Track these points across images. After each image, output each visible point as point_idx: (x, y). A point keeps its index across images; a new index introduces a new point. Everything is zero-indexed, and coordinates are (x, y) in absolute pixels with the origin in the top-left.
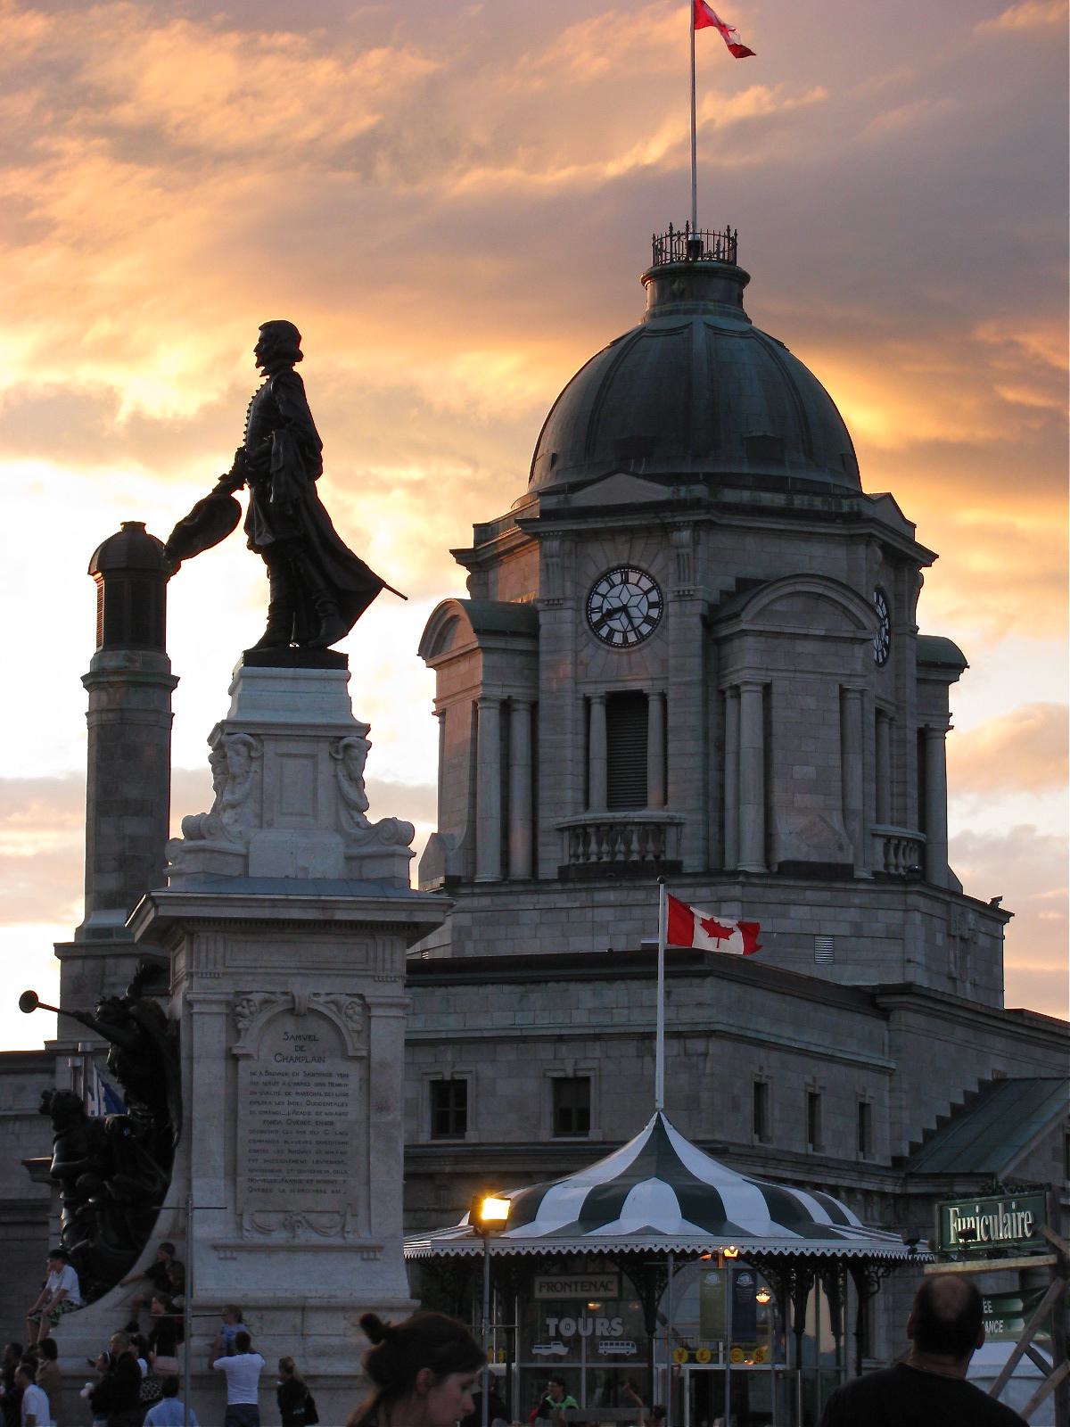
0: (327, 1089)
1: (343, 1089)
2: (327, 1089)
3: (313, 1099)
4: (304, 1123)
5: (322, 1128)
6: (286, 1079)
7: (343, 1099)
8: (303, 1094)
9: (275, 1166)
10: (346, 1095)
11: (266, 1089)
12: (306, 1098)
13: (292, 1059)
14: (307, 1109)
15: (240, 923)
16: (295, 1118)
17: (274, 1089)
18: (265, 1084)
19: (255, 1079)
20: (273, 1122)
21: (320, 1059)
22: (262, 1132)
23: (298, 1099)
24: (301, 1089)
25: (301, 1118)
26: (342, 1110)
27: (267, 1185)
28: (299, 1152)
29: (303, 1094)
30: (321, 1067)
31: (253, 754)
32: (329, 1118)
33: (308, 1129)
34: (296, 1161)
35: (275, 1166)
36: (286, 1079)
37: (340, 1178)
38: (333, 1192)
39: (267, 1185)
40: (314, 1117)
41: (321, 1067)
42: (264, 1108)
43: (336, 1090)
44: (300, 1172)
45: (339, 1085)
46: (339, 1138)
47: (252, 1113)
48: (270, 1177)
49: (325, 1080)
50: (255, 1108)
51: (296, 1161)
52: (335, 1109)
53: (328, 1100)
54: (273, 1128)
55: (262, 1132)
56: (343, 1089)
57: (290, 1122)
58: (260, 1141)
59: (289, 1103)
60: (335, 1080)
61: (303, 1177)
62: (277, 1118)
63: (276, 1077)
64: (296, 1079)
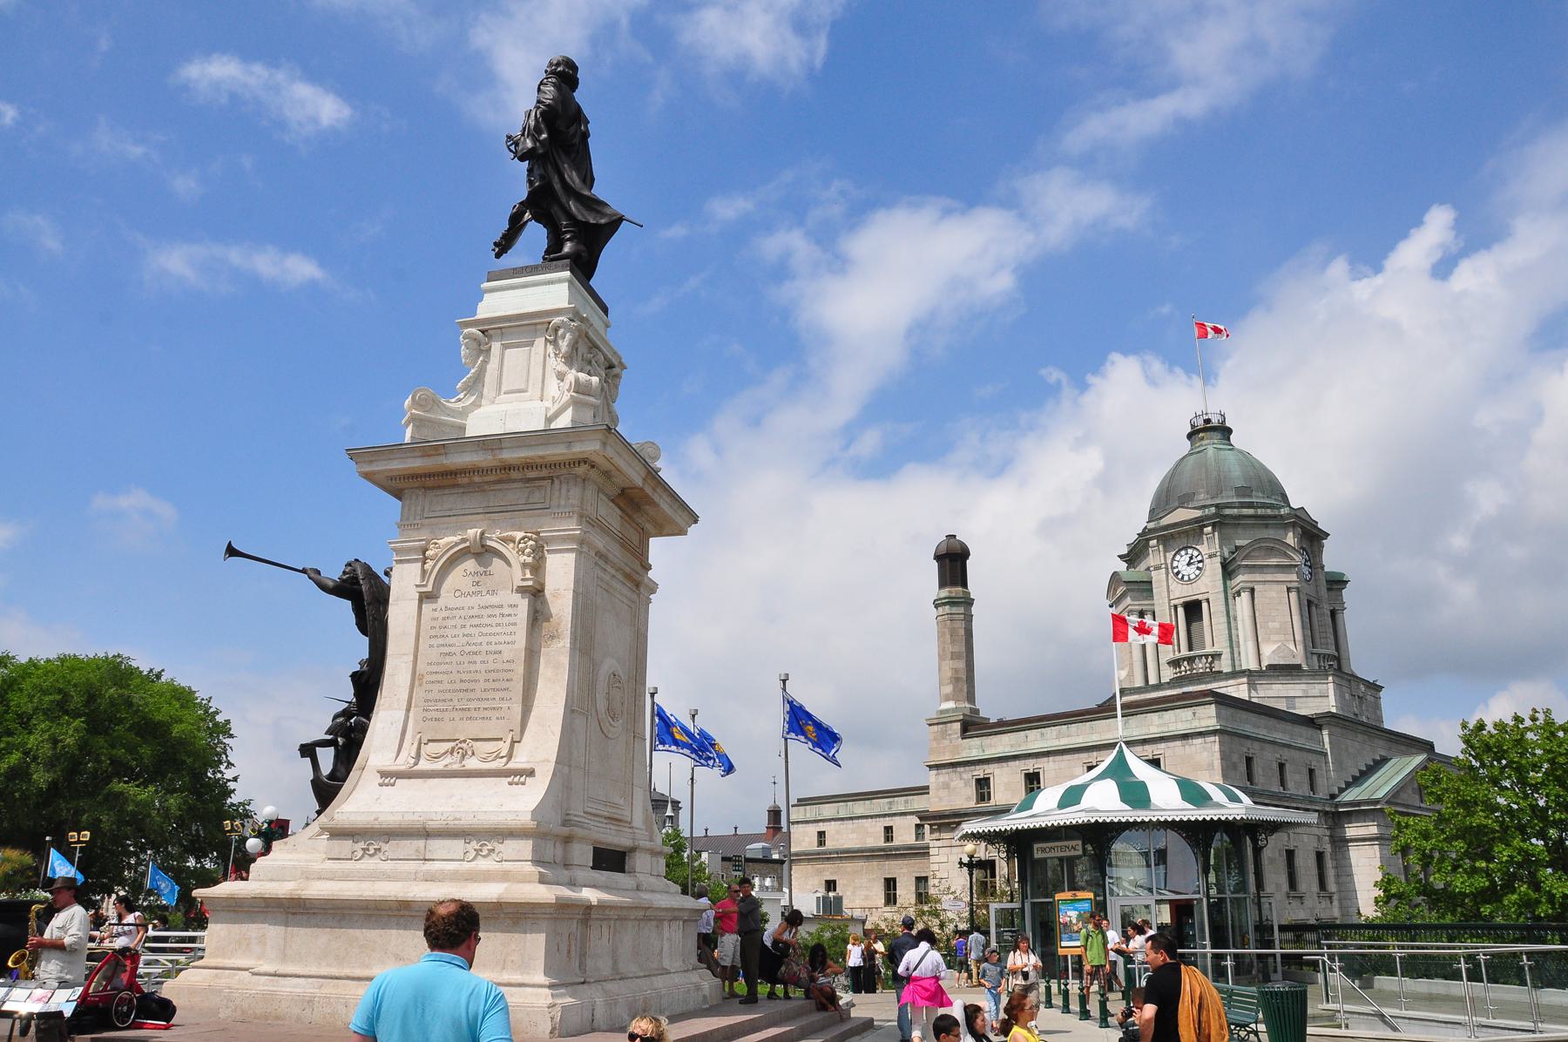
0: (498, 620)
1: (512, 619)
2: (498, 620)
3: (485, 630)
4: (475, 653)
5: (466, 659)
6: (462, 613)
7: (511, 628)
8: (476, 626)
9: (448, 696)
10: (515, 624)
11: (444, 623)
12: (479, 629)
13: (469, 594)
14: (480, 639)
15: (442, 476)
16: (467, 649)
17: (452, 622)
18: (444, 619)
19: (436, 614)
20: (449, 654)
21: (493, 592)
22: (439, 664)
23: (473, 631)
24: (475, 621)
25: (473, 648)
26: (508, 639)
27: (439, 715)
28: (470, 681)
29: (476, 626)
30: (494, 600)
31: (482, 348)
32: (499, 647)
33: (478, 658)
34: (466, 690)
35: (448, 696)
36: (462, 613)
37: (505, 705)
38: (498, 718)
39: (439, 715)
40: (485, 648)
41: (494, 600)
42: (441, 641)
43: (506, 620)
44: (469, 700)
45: (510, 615)
46: (506, 666)
47: (431, 646)
48: (440, 706)
49: (497, 611)
50: (433, 642)
51: (466, 690)
52: (502, 638)
53: (499, 630)
54: (448, 659)
55: (439, 664)
56: (512, 619)
57: (462, 653)
58: (436, 673)
59: (464, 635)
60: (506, 611)
61: (472, 705)
62: (452, 649)
63: (454, 612)
64: (471, 613)
